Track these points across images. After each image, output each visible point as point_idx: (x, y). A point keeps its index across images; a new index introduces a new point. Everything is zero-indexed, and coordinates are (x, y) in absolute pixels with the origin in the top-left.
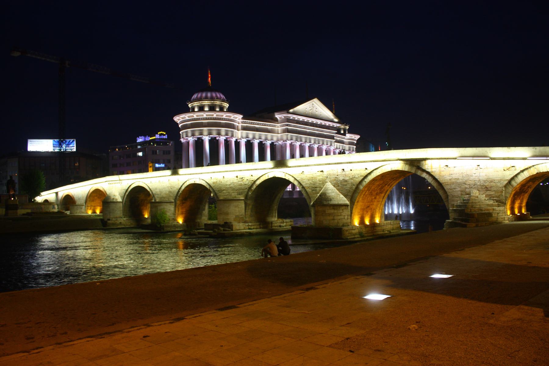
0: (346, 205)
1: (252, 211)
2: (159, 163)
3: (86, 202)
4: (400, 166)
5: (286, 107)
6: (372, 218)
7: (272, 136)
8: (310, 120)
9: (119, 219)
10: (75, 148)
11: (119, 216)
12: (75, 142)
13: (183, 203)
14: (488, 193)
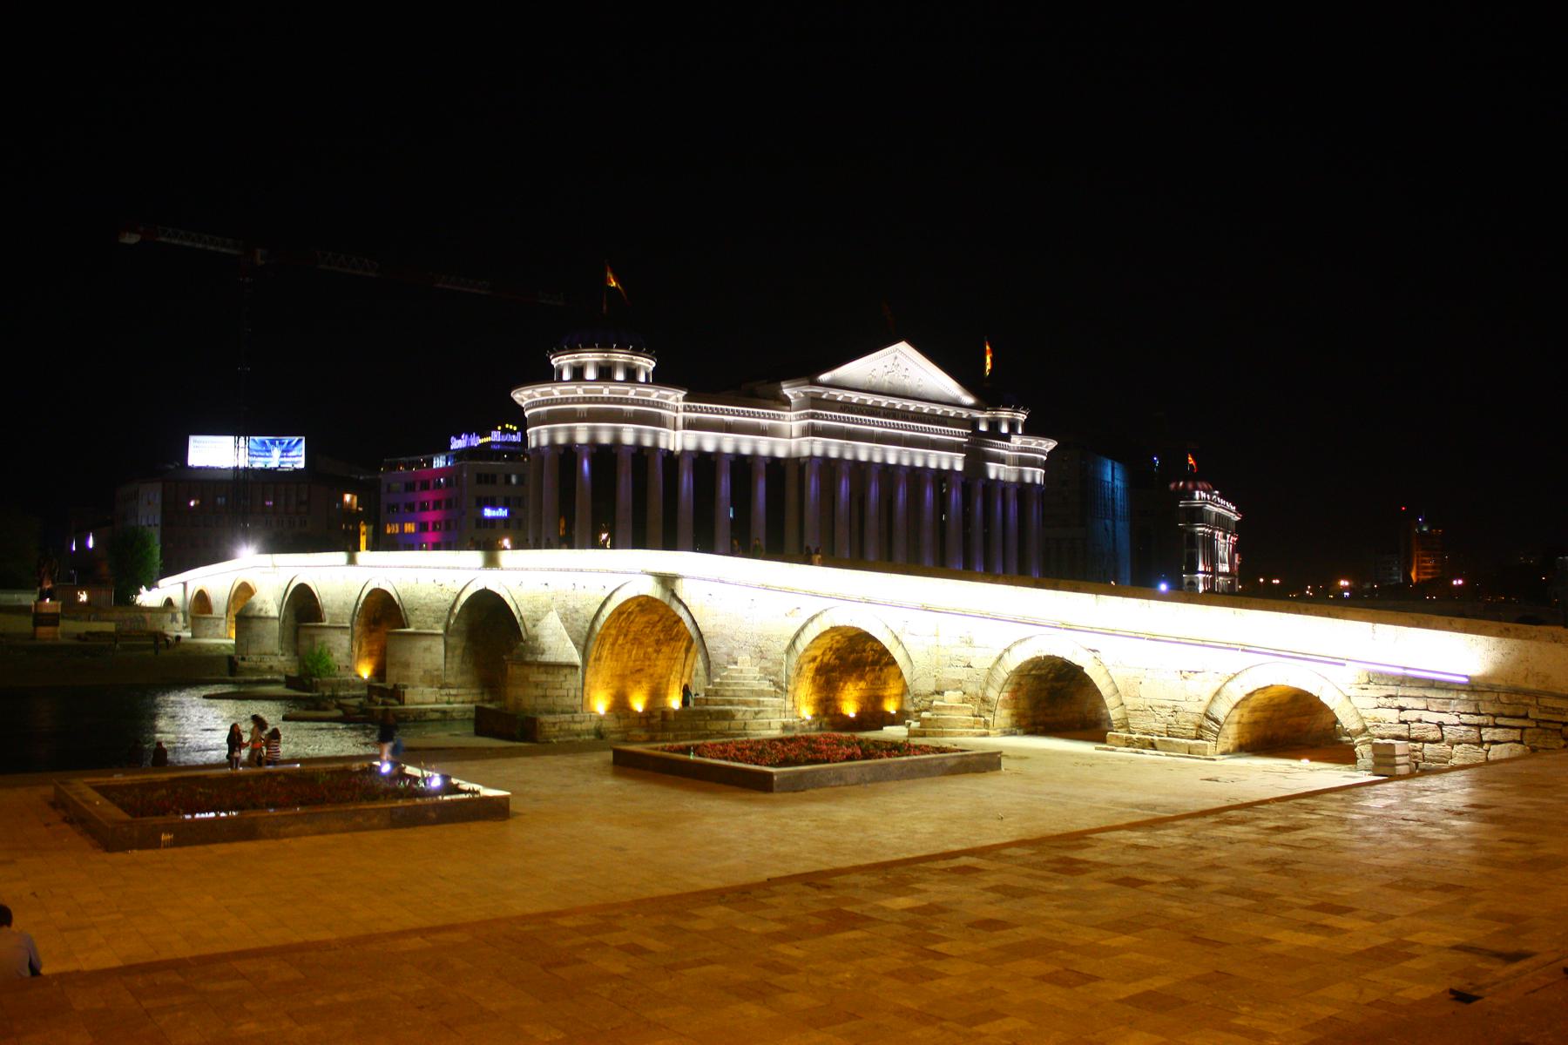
0: (574, 667)
1: (463, 662)
2: (494, 507)
3: (228, 611)
4: (652, 589)
5: (807, 371)
6: (656, 695)
7: (773, 445)
8: (885, 402)
9: (267, 658)
10: (303, 459)
11: (273, 654)
12: (303, 444)
13: (371, 631)
14: (765, 664)
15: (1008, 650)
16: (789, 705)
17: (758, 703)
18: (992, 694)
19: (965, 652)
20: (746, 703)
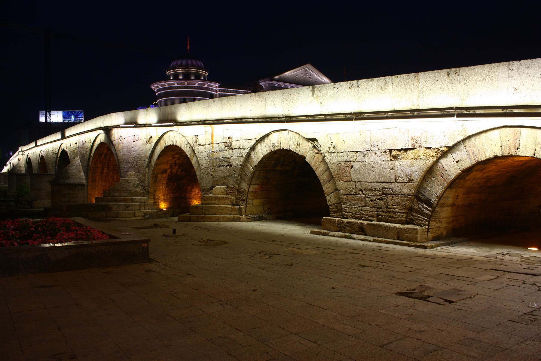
0: (82, 185)
15: (253, 148)
16: (151, 201)
17: (132, 200)
18: (244, 186)
19: (227, 154)
20: (125, 200)
